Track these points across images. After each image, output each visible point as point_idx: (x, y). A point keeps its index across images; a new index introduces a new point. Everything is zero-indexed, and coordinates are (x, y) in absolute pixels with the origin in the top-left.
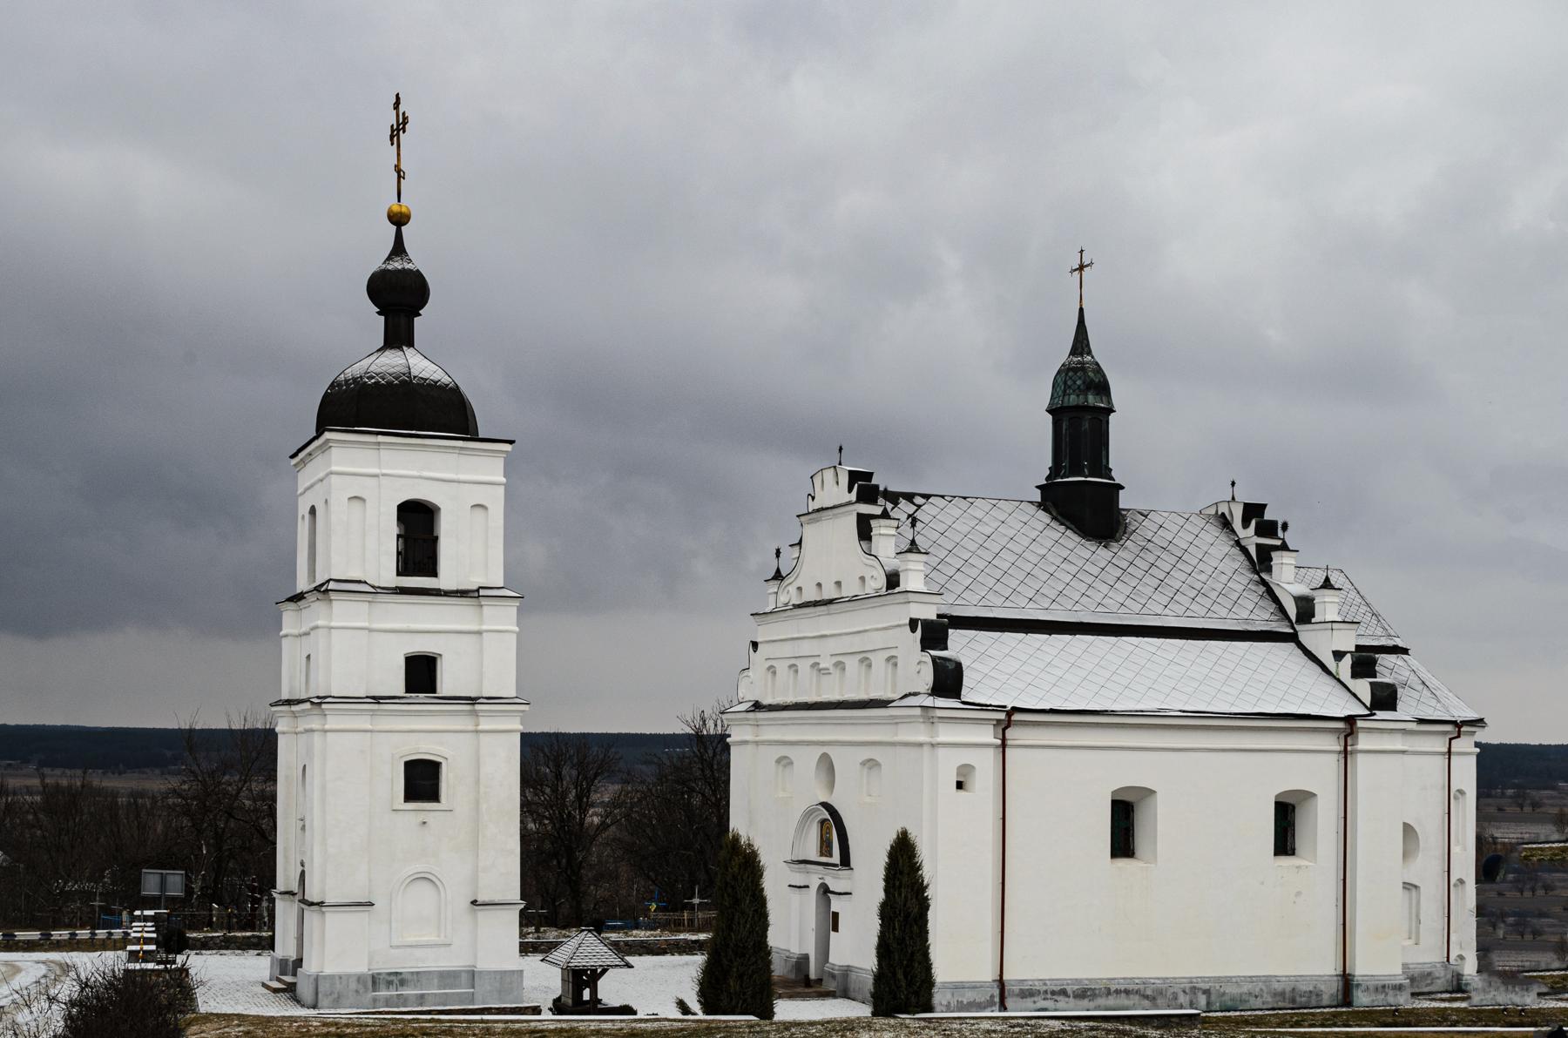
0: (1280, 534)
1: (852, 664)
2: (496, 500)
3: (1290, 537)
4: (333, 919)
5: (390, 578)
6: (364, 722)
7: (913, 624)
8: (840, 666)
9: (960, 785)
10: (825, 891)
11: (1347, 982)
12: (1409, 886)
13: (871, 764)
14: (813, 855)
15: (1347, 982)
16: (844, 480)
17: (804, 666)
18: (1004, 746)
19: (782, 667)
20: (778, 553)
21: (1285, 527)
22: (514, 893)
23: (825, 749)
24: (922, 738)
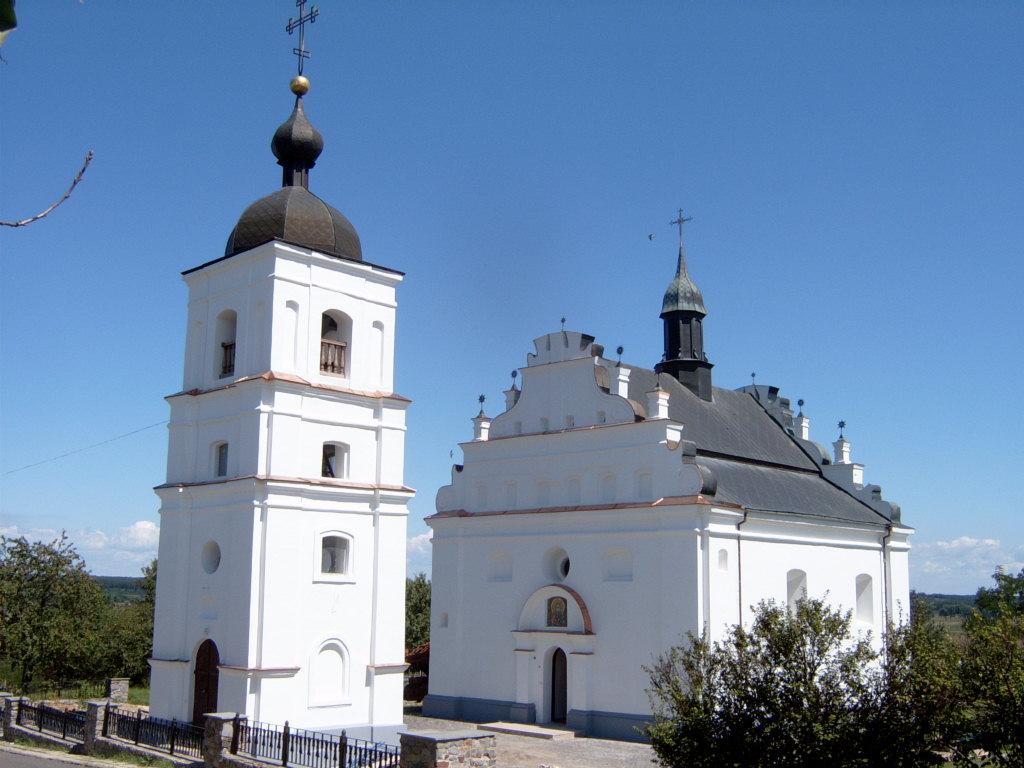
2: (389, 318)
20: (482, 399)
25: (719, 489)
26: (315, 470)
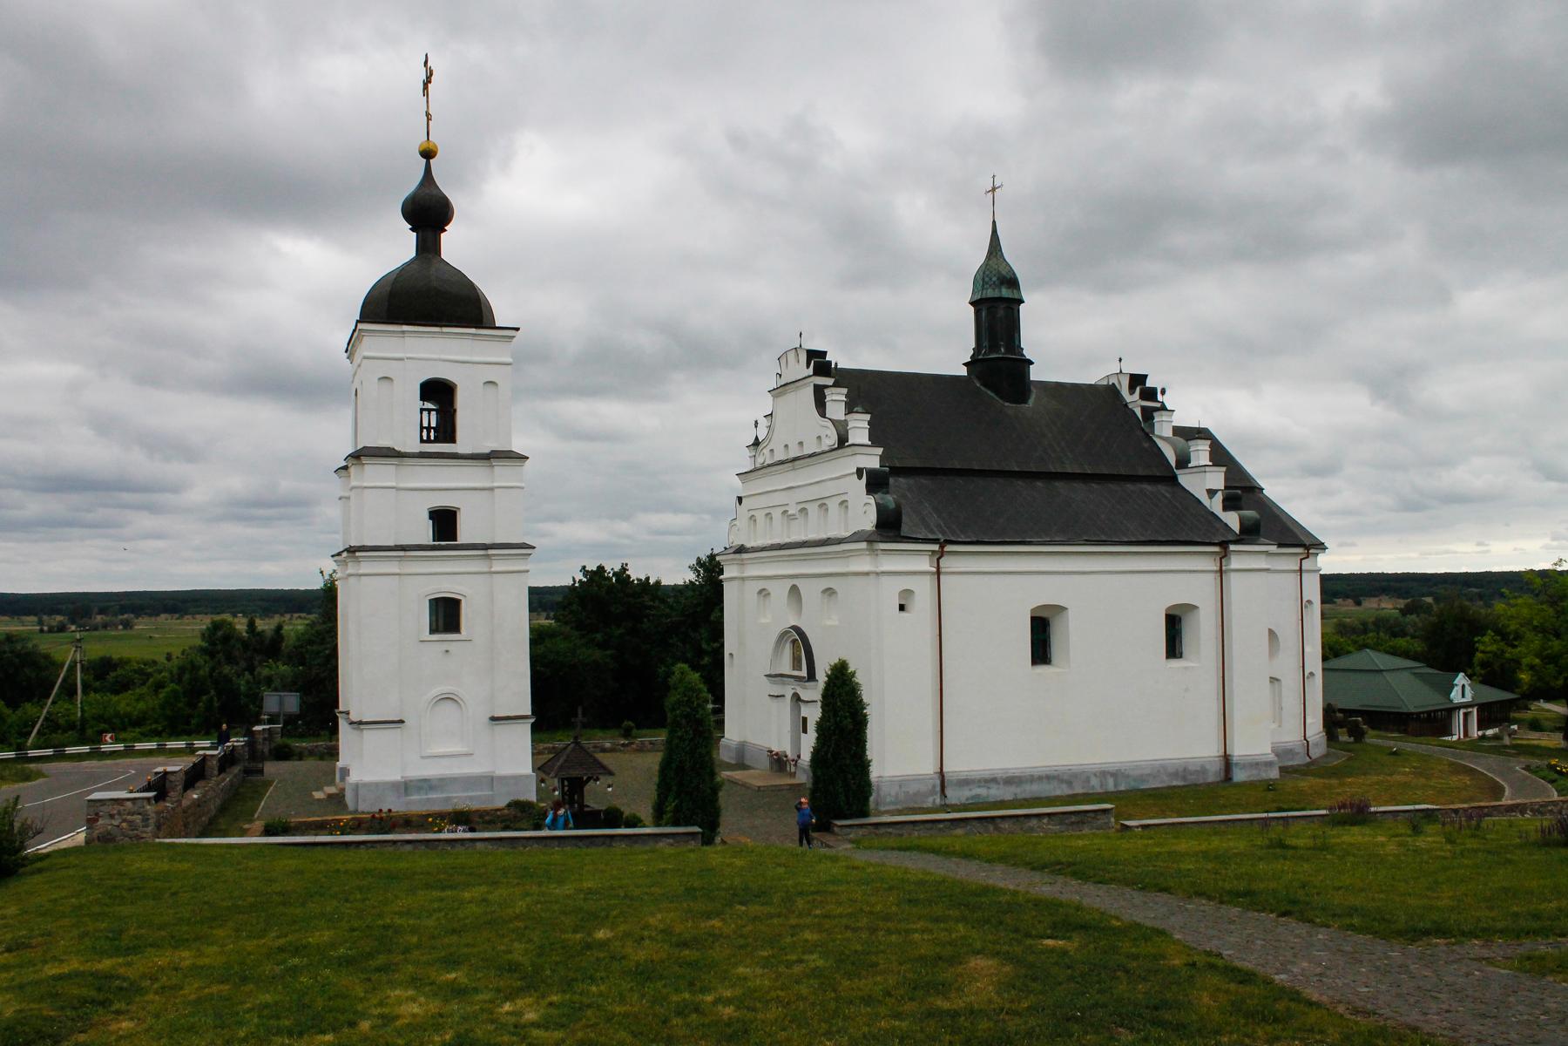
0: (1160, 398)
1: (813, 509)
3: (1167, 400)
4: (370, 735)
5: (414, 446)
6: (393, 567)
7: (859, 472)
9: (902, 608)
10: (797, 698)
11: (1227, 761)
12: (1273, 680)
13: (829, 592)
14: (786, 667)
15: (1227, 761)
16: (803, 358)
17: (777, 513)
18: (938, 573)
19: (760, 515)
21: (1163, 392)
22: (527, 709)
23: (795, 582)
24: (866, 568)
25: (905, 519)
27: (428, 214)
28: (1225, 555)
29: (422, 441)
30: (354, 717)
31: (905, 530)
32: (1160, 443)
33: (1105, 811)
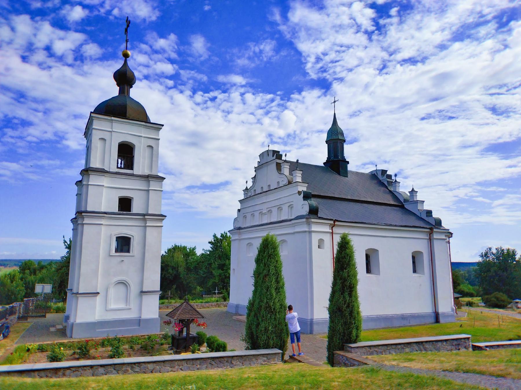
0: (393, 178)
1: (275, 210)
5: (114, 169)
7: (299, 193)
8: (270, 211)
16: (271, 154)
18: (332, 233)
19: (249, 216)
21: (396, 175)
22: (157, 287)
26: (116, 209)
27: (125, 79)
28: (431, 233)
29: (118, 168)
30: (75, 291)
31: (319, 215)
32: (395, 193)
33: (468, 338)
